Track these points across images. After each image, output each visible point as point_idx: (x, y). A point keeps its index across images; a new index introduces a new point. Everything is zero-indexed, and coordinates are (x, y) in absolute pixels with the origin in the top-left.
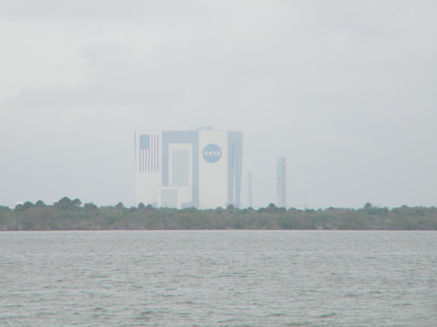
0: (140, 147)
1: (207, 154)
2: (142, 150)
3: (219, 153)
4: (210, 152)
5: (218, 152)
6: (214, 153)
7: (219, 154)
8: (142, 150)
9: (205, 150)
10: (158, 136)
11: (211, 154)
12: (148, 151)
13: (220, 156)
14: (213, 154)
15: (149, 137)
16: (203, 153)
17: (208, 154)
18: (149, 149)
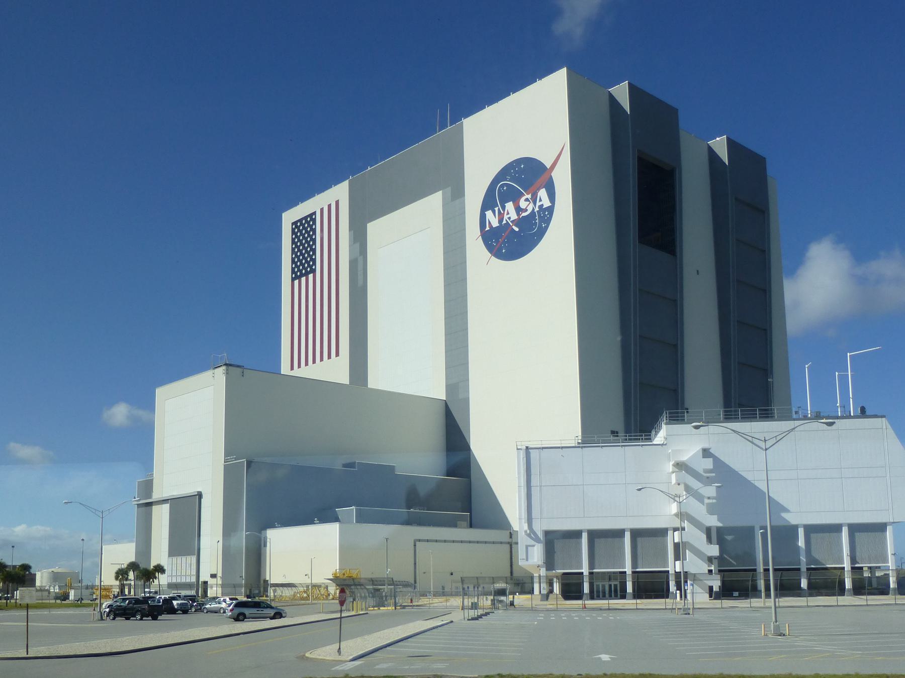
0: (293, 272)
1: (495, 223)
2: (296, 282)
4: (510, 206)
5: (543, 193)
6: (523, 204)
7: (546, 203)
8: (296, 282)
10: (337, 203)
11: (514, 216)
12: (311, 276)
13: (551, 210)
14: (518, 210)
15: (314, 221)
17: (501, 221)
18: (313, 271)
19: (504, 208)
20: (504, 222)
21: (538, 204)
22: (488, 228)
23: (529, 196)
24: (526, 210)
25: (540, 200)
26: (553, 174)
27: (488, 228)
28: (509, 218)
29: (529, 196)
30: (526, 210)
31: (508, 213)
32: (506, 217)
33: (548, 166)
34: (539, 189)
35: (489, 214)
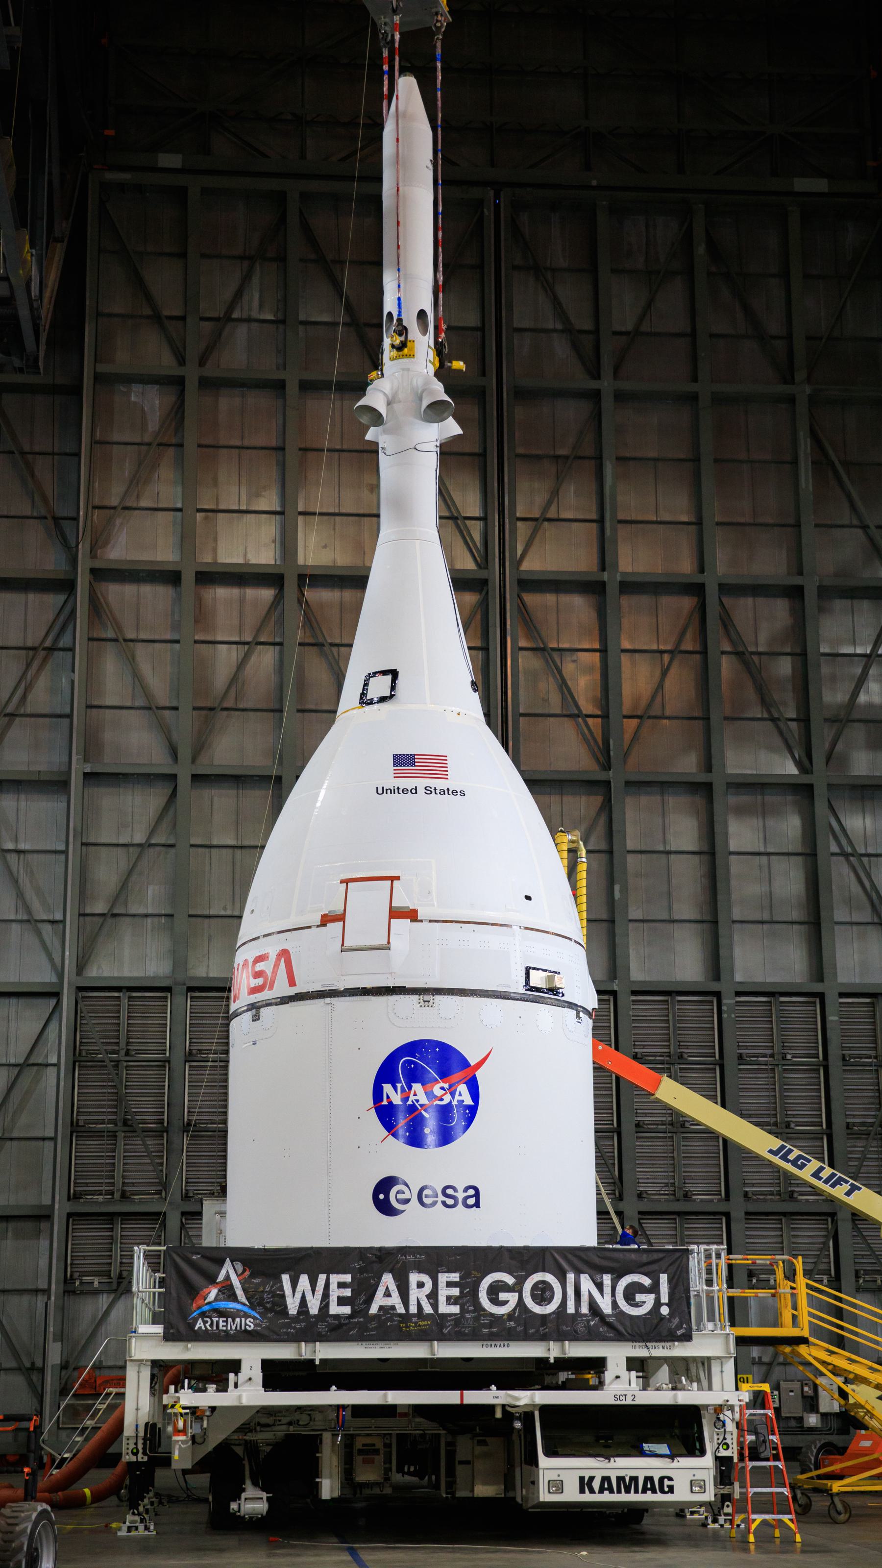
3: (463, 1094)
5: (463, 1088)
6: (437, 1091)
7: (469, 1101)
9: (387, 1073)
11: (423, 1100)
16: (378, 1093)
19: (410, 1088)
20: (410, 1102)
21: (457, 1098)
22: (385, 1102)
23: (446, 1086)
24: (442, 1100)
25: (460, 1095)
26: (479, 1074)
27: (385, 1102)
28: (417, 1101)
29: (446, 1086)
30: (442, 1100)
31: (415, 1095)
32: (412, 1098)
33: (473, 1062)
34: (459, 1082)
35: (387, 1088)
